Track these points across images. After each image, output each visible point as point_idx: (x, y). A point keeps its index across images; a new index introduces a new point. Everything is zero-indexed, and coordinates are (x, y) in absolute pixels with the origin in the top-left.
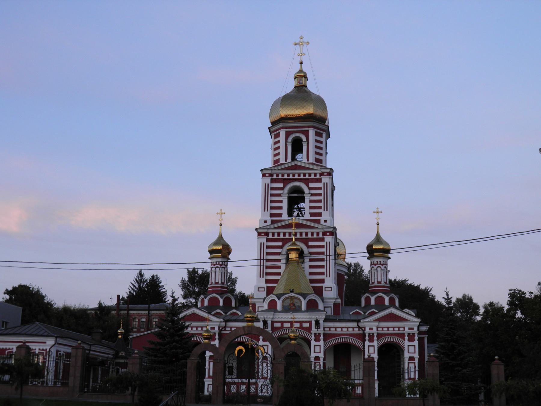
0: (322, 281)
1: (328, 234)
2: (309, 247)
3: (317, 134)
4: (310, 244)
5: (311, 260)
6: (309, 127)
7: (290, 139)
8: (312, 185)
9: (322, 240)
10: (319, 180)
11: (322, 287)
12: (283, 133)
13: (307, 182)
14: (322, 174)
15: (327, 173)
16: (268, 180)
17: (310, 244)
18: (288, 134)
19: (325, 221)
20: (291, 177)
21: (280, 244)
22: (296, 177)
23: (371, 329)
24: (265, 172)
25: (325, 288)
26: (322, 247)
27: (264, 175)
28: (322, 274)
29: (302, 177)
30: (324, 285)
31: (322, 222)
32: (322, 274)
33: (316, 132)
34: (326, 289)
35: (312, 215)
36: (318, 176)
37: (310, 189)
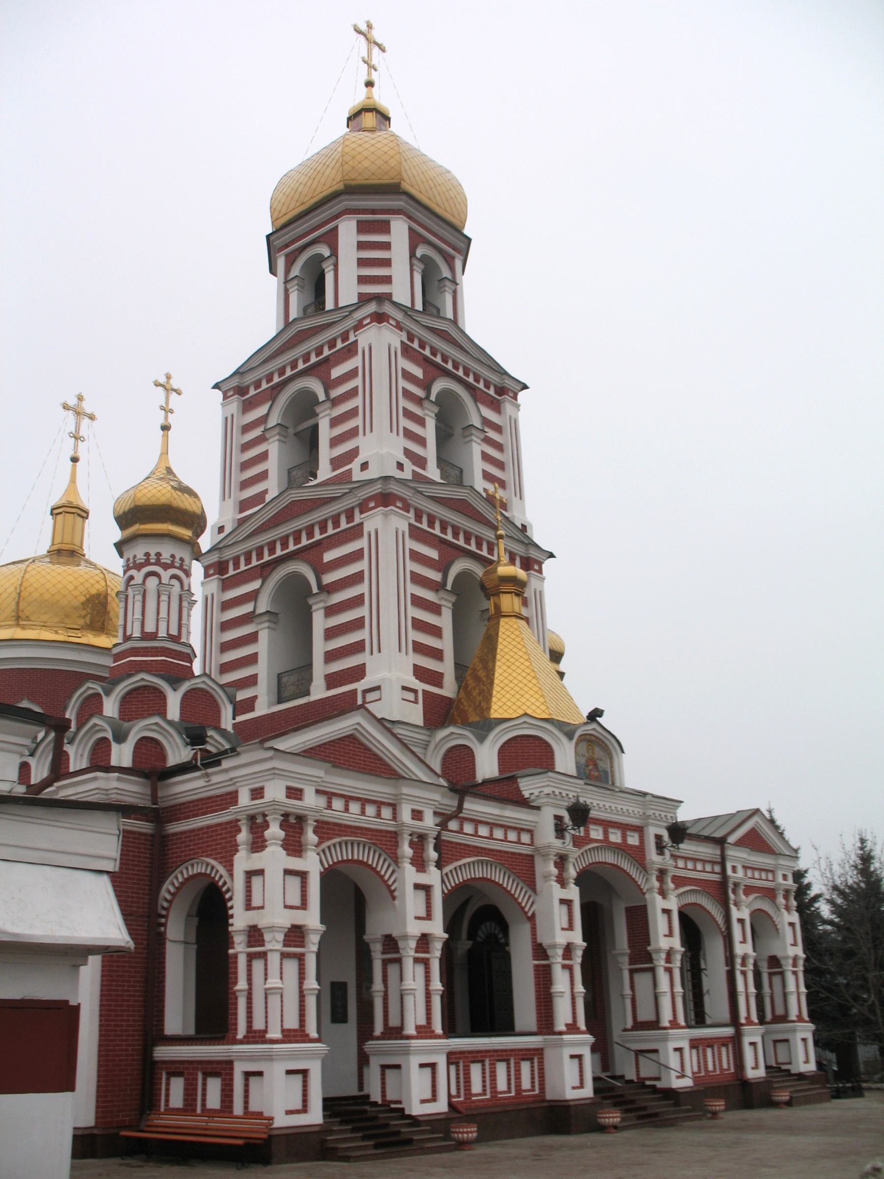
0: (359, 672)
1: (372, 504)
2: (320, 569)
3: (363, 227)
4: (329, 556)
5: (330, 611)
6: (337, 216)
7: (296, 271)
8: (336, 372)
9: (356, 532)
10: (351, 350)
11: (355, 691)
12: (281, 263)
13: (320, 369)
14: (359, 326)
15: (370, 315)
16: (234, 406)
17: (329, 556)
18: (290, 261)
19: (364, 466)
20: (289, 373)
21: (255, 585)
22: (301, 366)
23: (417, 815)
24: (225, 387)
25: (365, 692)
26: (357, 556)
27: (225, 397)
28: (359, 647)
29: (314, 359)
30: (360, 686)
31: (358, 475)
32: (359, 647)
33: (359, 222)
34: (370, 697)
35: (336, 463)
36: (352, 338)
37: (329, 385)
